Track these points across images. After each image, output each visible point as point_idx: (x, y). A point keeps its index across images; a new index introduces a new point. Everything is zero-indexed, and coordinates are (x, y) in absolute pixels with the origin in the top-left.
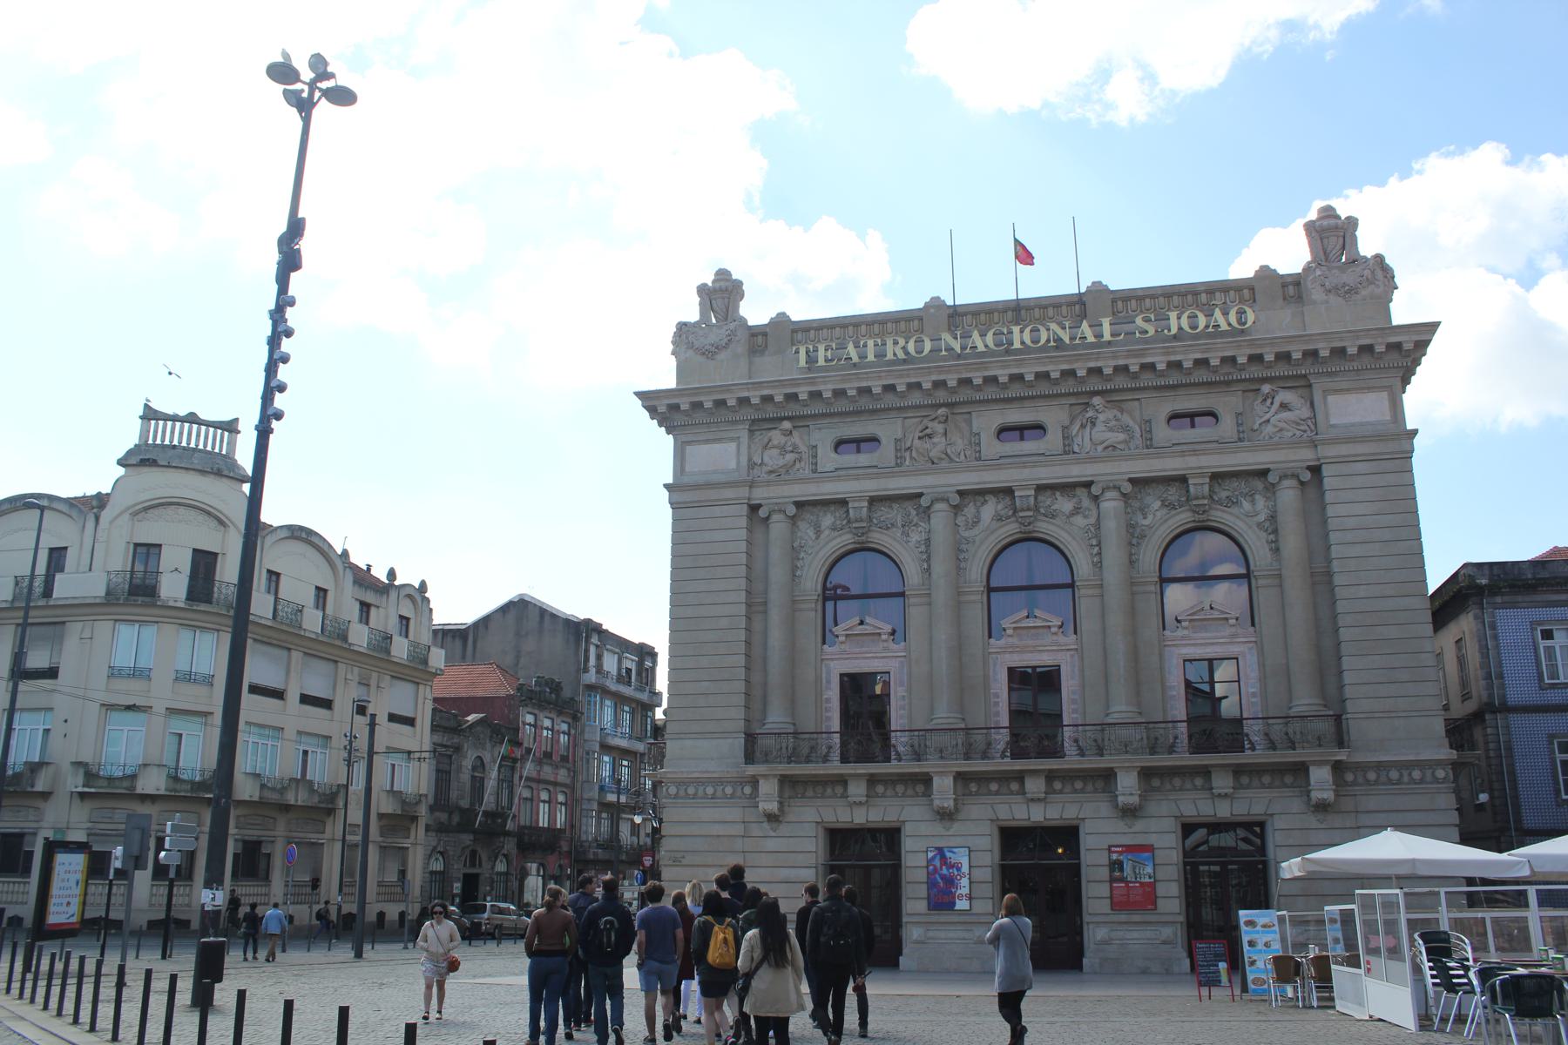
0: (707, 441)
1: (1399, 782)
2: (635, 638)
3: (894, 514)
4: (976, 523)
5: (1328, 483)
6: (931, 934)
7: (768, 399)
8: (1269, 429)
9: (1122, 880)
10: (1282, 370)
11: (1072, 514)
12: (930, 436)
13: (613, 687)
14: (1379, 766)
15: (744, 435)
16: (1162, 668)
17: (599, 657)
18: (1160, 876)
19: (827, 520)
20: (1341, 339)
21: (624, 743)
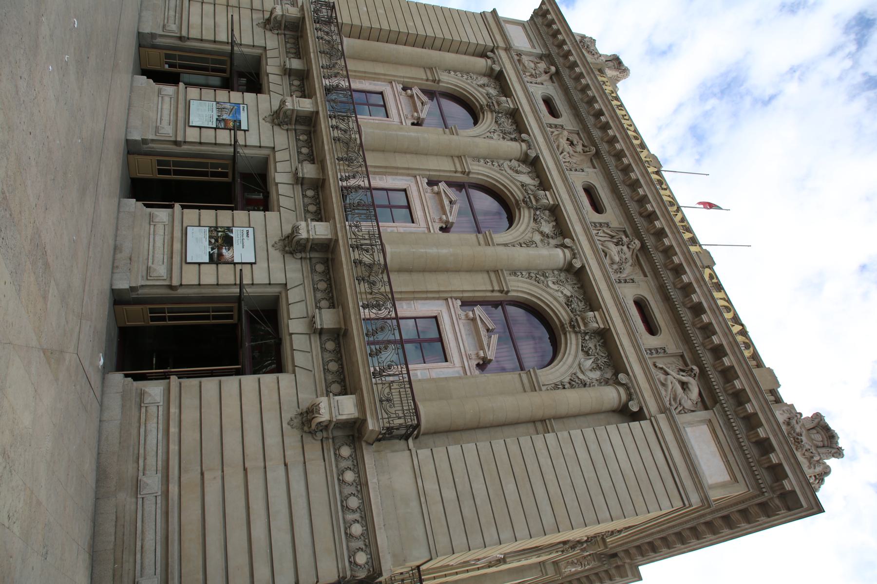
1: (346, 508)
3: (508, 125)
4: (517, 172)
5: (635, 425)
6: (167, 99)
8: (662, 377)
10: (715, 378)
11: (541, 233)
12: (572, 144)
14: (362, 485)
15: (538, 51)
19: (493, 92)
20: (768, 420)
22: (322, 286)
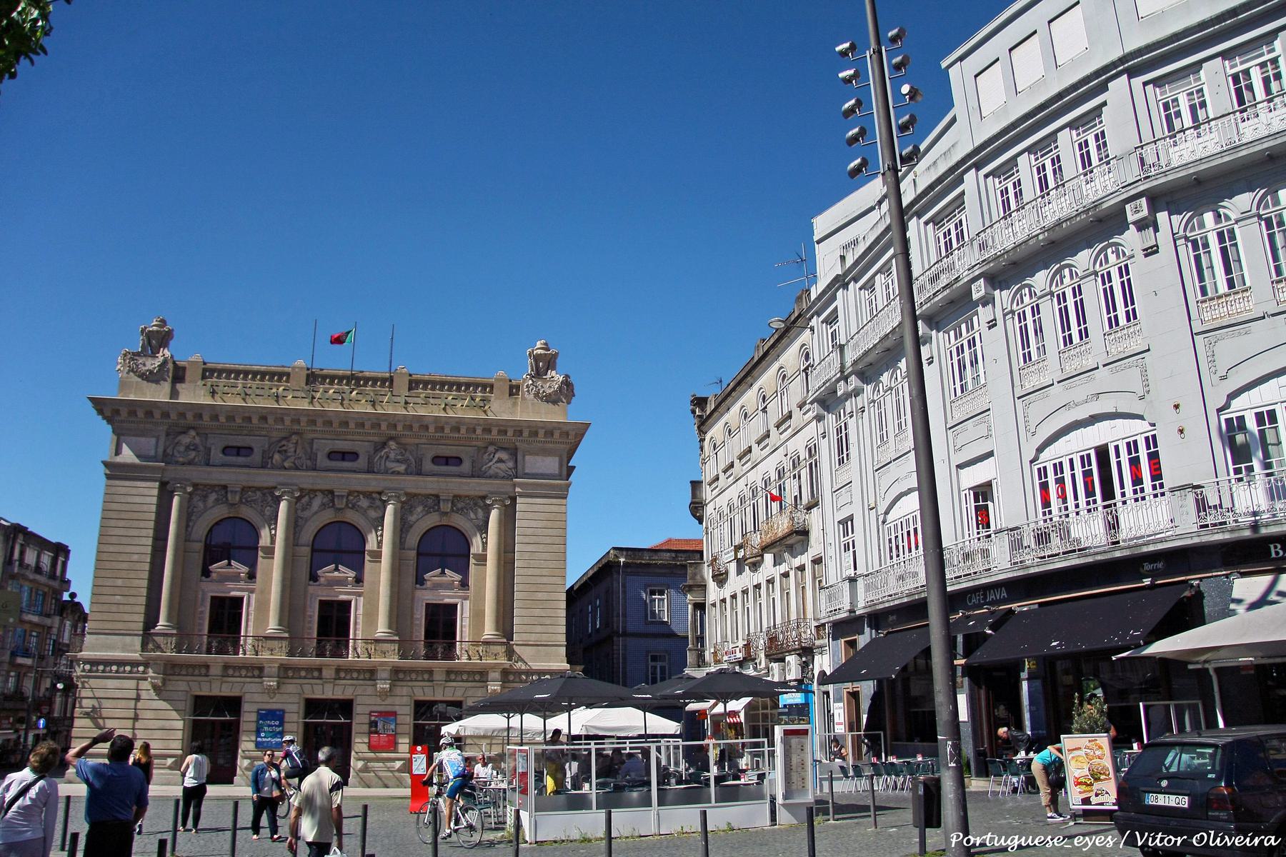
2: (54, 539)
7: (182, 415)
9: (376, 732)
13: (31, 577)
16: (412, 608)
17: (22, 553)
18: (399, 730)
21: (35, 619)
22: (414, 676)
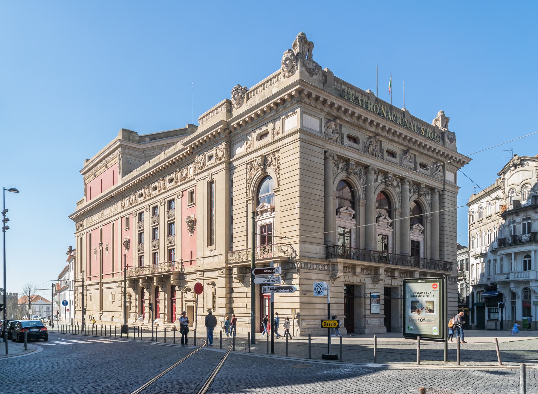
0: (310, 115)
11: (396, 187)
